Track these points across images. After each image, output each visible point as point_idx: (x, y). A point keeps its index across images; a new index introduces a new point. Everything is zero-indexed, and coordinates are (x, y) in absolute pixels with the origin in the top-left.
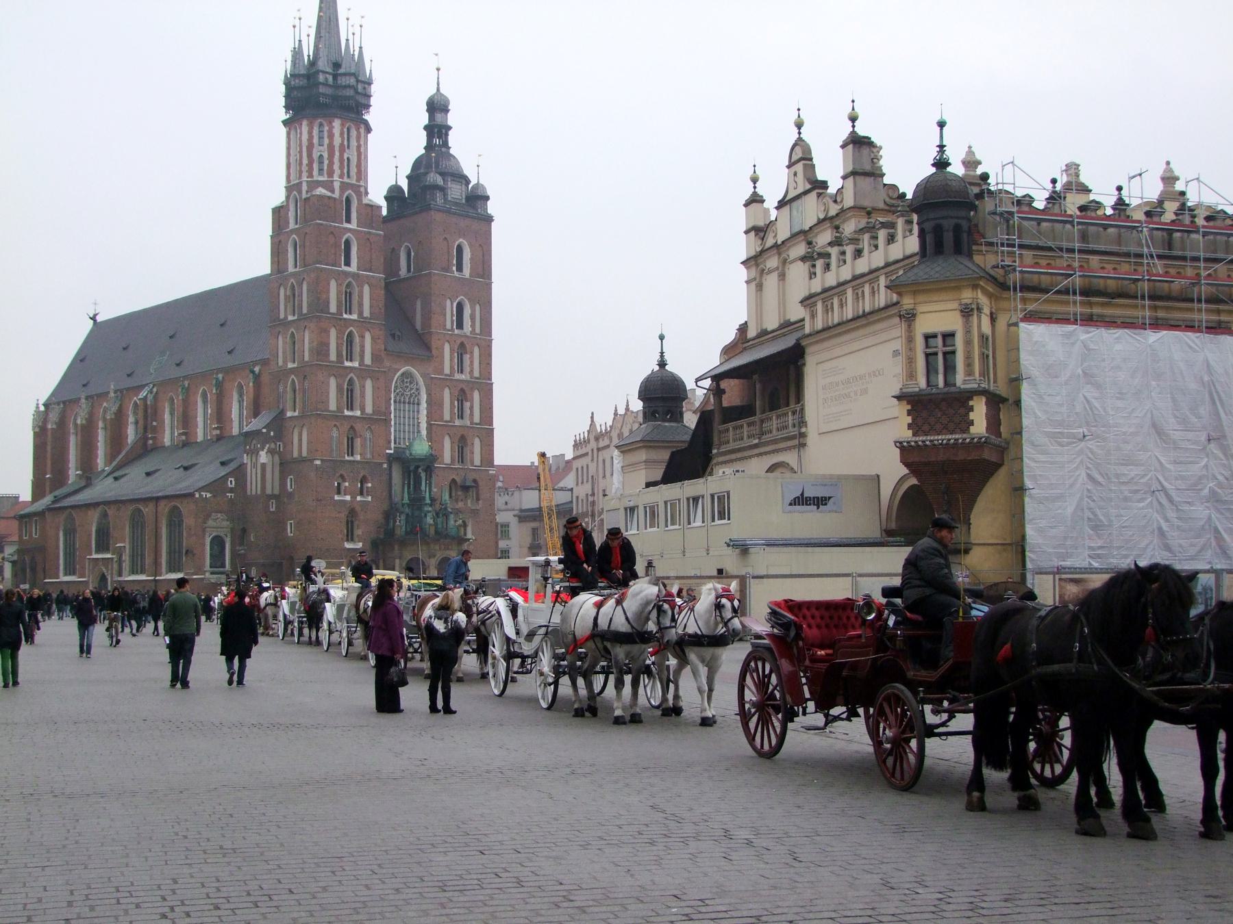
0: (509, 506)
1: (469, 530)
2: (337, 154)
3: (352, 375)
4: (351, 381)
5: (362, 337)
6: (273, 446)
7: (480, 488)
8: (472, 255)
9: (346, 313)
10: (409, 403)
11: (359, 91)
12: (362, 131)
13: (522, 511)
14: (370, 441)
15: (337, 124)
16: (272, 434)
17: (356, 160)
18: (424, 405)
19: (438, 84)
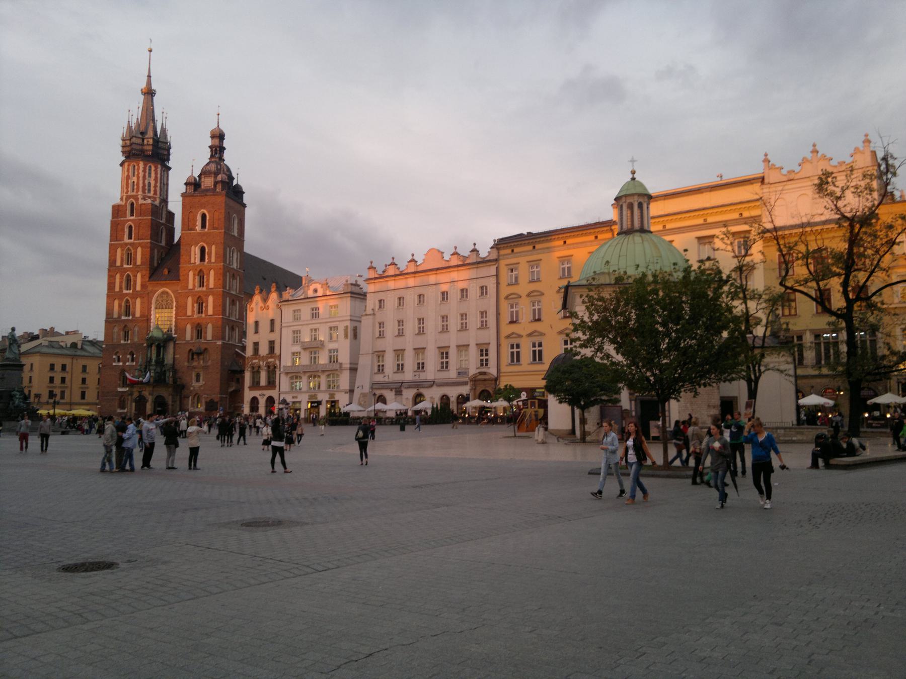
3: (127, 297)
4: (127, 301)
5: (135, 276)
8: (210, 217)
9: (128, 264)
14: (138, 332)
19: (218, 123)
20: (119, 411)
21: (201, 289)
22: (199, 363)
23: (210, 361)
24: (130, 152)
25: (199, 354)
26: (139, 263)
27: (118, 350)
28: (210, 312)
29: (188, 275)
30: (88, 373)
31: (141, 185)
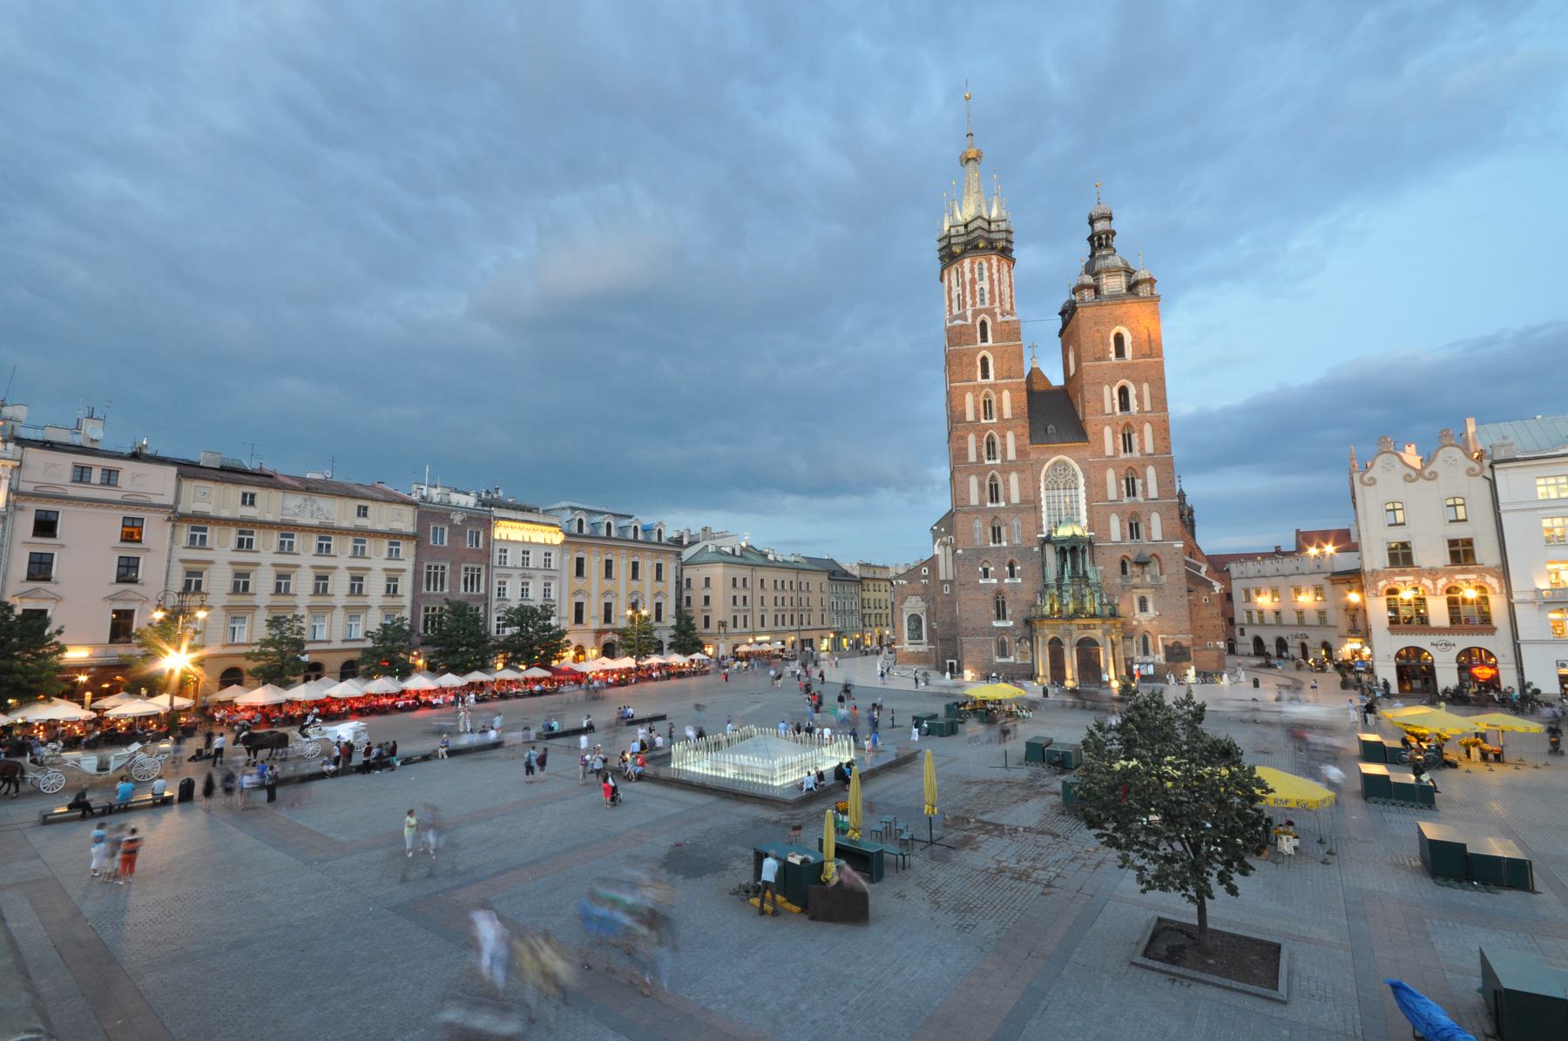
0: (1322, 570)
1: (1150, 606)
2: (968, 287)
3: (994, 471)
5: (1003, 437)
6: (945, 539)
7: (1163, 562)
9: (986, 418)
10: (1065, 489)
11: (993, 230)
12: (994, 259)
13: (1334, 574)
14: (1018, 528)
15: (967, 262)
16: (943, 530)
17: (988, 287)
18: (1082, 489)
20: (999, 660)
21: (1128, 455)
22: (1144, 580)
23: (1164, 577)
24: (966, 244)
25: (1142, 564)
26: (1007, 414)
27: (986, 558)
28: (1153, 492)
29: (1103, 433)
30: (766, 590)
31: (997, 293)
